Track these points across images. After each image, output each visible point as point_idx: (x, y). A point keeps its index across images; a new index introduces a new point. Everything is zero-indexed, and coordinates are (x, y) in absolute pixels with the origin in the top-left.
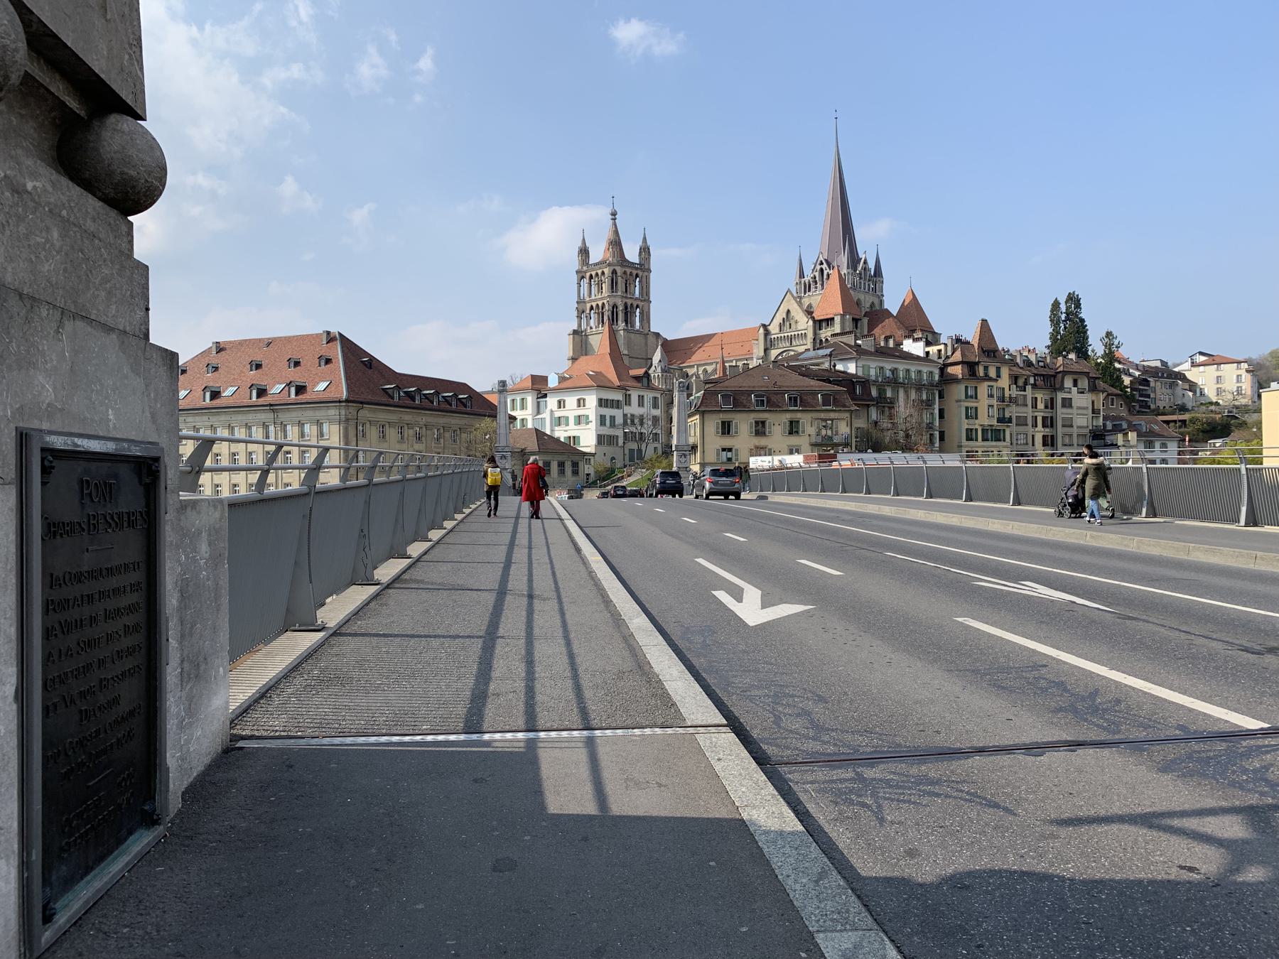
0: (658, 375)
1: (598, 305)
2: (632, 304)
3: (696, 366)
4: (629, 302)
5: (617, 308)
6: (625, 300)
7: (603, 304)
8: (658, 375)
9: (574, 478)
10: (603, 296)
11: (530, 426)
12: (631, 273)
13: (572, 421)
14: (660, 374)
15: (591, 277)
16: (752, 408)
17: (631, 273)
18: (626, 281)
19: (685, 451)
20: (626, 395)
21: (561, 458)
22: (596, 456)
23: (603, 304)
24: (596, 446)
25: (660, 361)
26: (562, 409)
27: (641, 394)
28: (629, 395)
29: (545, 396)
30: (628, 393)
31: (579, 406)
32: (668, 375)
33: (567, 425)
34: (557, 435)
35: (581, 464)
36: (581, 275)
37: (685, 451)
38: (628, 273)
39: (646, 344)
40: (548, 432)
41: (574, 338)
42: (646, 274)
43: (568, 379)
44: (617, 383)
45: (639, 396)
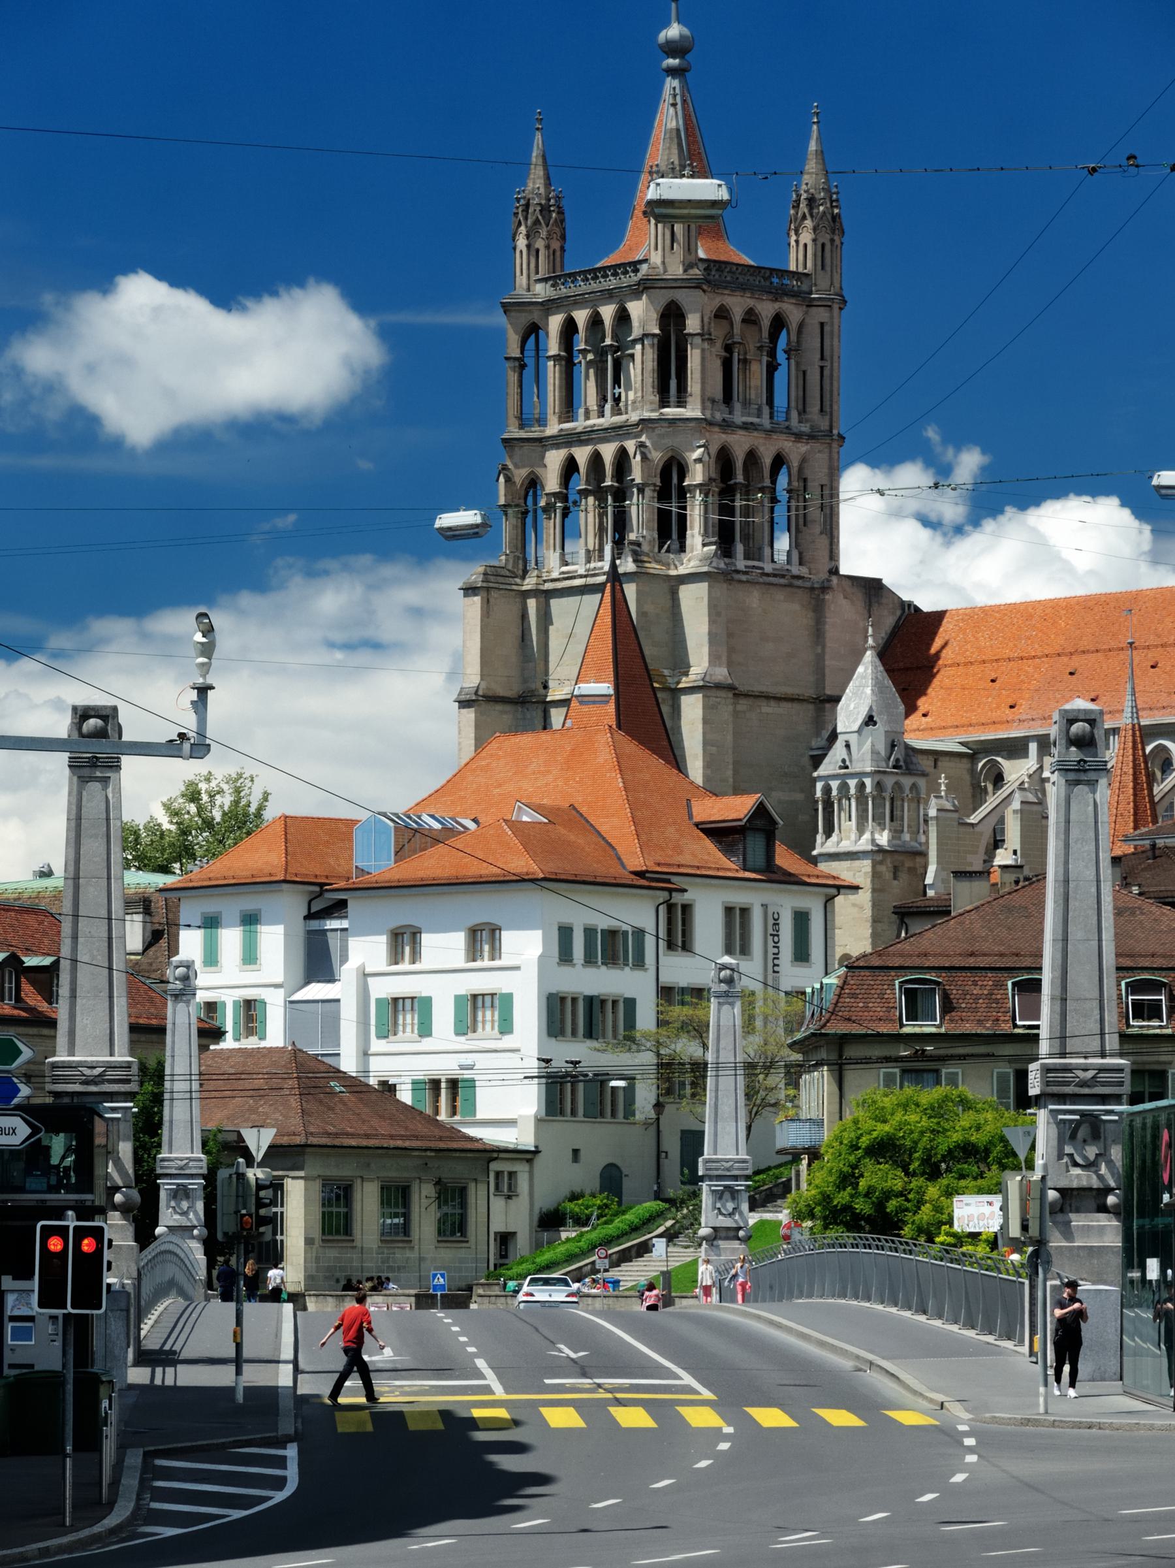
0: (862, 786)
1: (596, 460)
2: (752, 457)
3: (1033, 747)
4: (740, 444)
5: (682, 475)
6: (719, 438)
7: (622, 458)
8: (862, 786)
9: (447, 1254)
10: (618, 419)
11: (275, 1035)
12: (751, 318)
13: (444, 1016)
14: (868, 782)
15: (570, 328)
16: (1006, 1028)
17: (751, 318)
18: (728, 348)
19: (736, 1178)
20: (671, 908)
21: (394, 1171)
22: (539, 1161)
23: (622, 458)
24: (539, 1121)
25: (870, 720)
26: (405, 966)
27: (739, 897)
28: (687, 909)
29: (338, 908)
30: (678, 898)
31: (473, 953)
32: (907, 782)
33: (425, 1030)
34: (380, 1069)
35: (477, 1196)
36: (524, 319)
37: (736, 1178)
38: (738, 315)
39: (818, 633)
40: (348, 1064)
41: (487, 603)
42: (821, 314)
43: (434, 839)
44: (636, 862)
45: (729, 910)
